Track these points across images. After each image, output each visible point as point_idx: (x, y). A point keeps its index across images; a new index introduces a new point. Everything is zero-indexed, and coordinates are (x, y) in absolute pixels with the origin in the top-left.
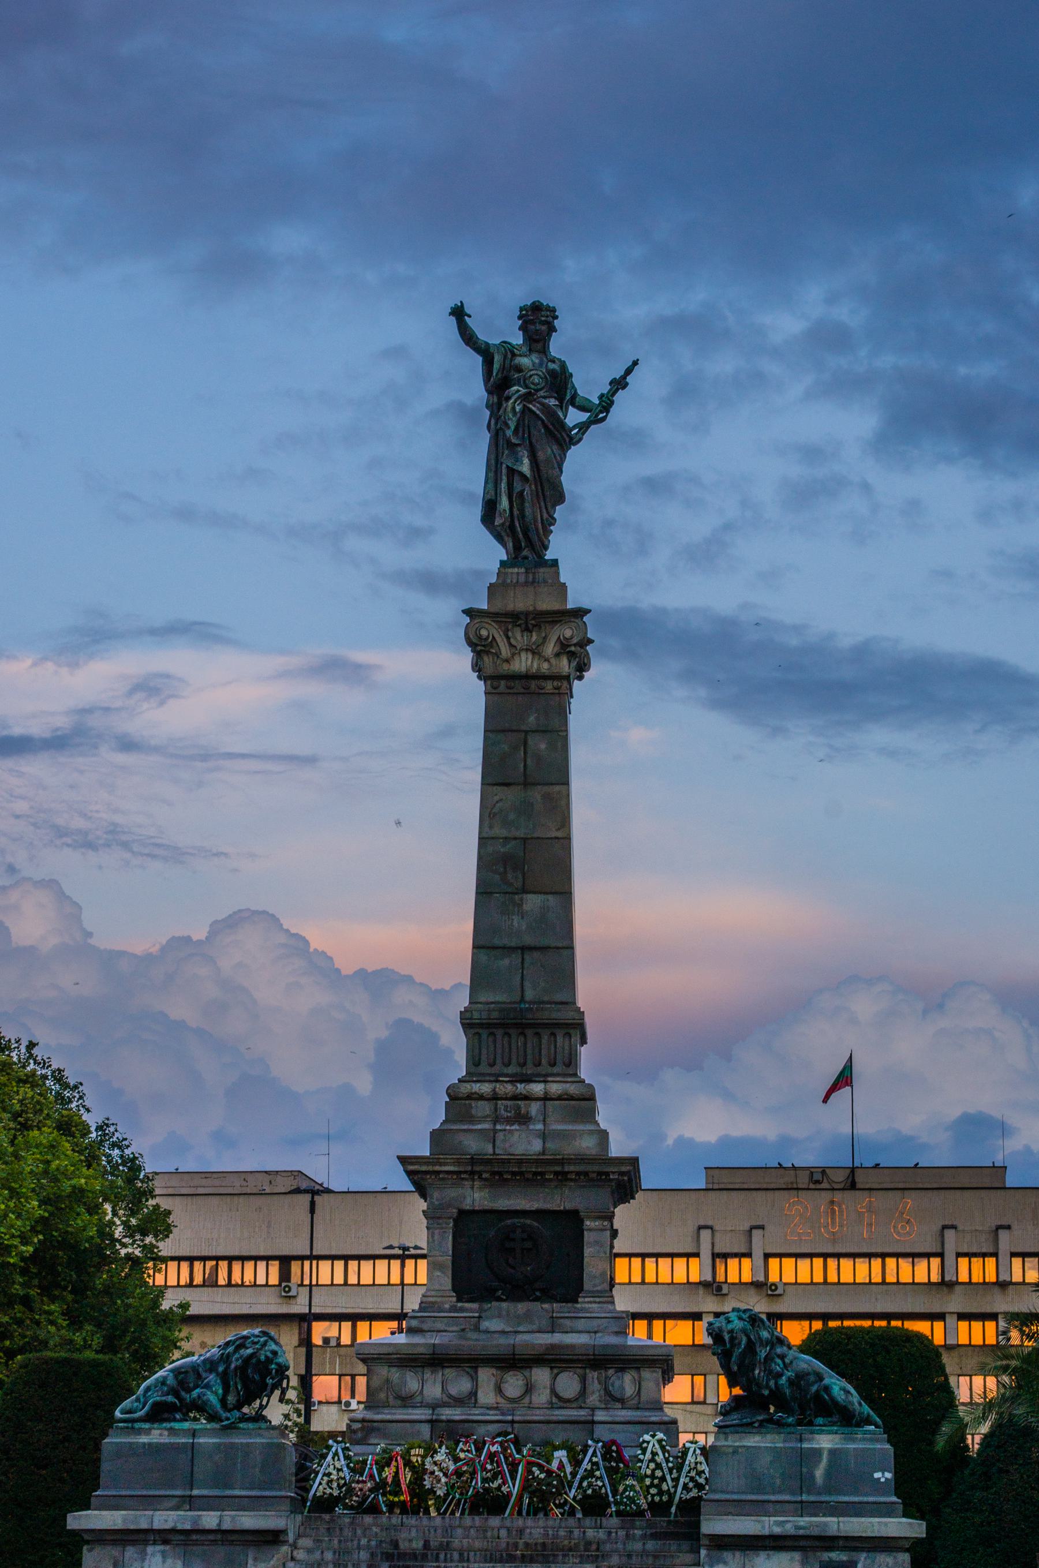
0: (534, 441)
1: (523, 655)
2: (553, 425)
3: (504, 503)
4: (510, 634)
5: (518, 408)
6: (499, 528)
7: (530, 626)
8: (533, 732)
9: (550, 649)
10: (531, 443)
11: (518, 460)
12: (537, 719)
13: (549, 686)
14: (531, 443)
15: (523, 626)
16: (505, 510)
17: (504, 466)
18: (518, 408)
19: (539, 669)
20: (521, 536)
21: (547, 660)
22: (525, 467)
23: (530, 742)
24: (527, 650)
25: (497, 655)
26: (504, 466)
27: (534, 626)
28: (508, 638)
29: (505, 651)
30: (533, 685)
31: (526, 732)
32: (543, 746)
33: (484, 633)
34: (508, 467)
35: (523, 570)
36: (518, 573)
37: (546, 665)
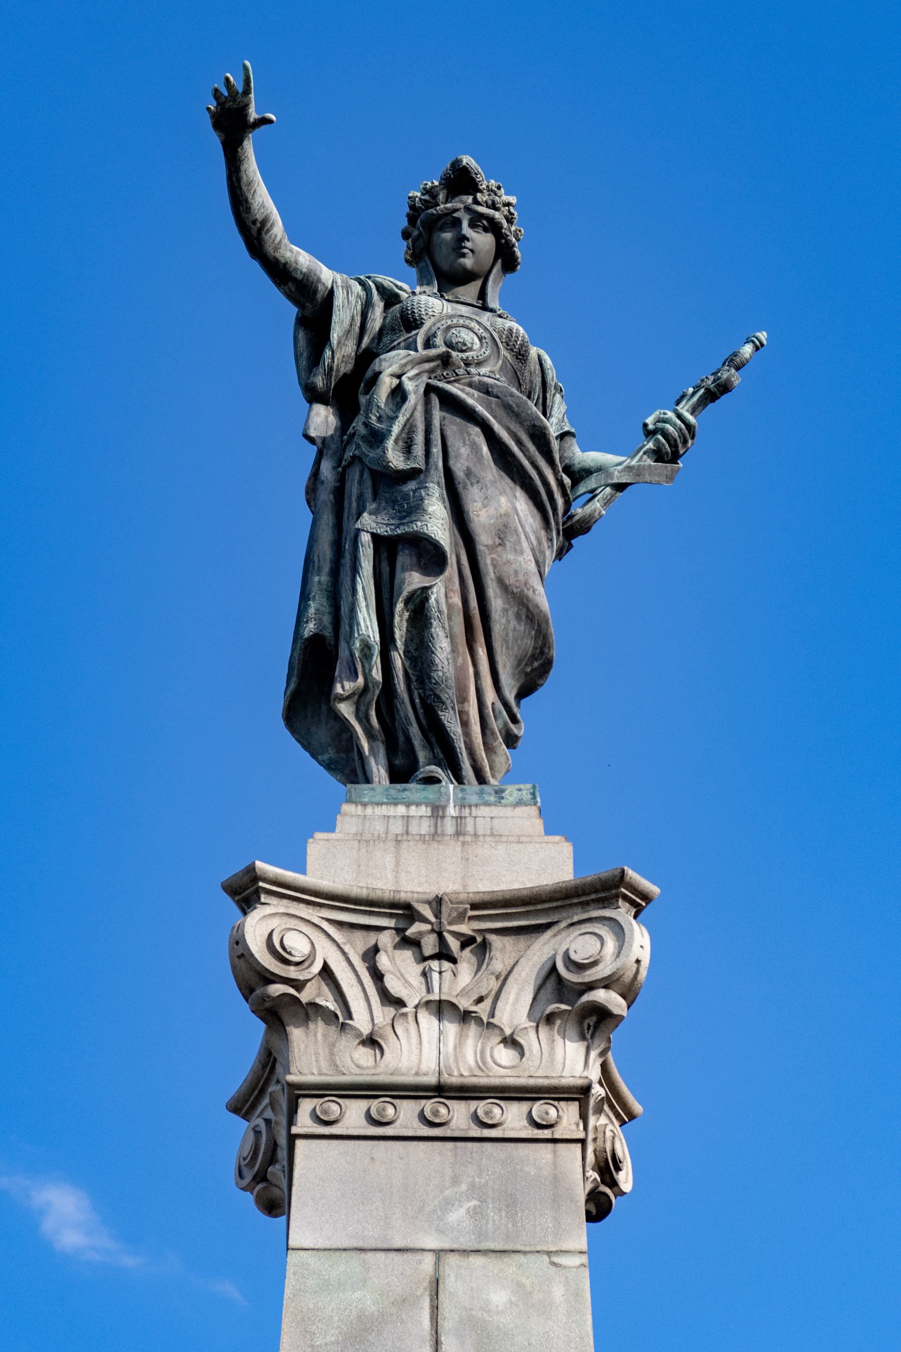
0: (458, 468)
1: (428, 1021)
2: (519, 442)
3: (367, 624)
4: (383, 961)
5: (413, 387)
6: (346, 710)
7: (454, 944)
8: (465, 1252)
9: (515, 1008)
10: (449, 474)
11: (413, 509)
12: (476, 1214)
13: (513, 1118)
14: (449, 474)
15: (430, 945)
16: (367, 647)
17: (366, 538)
18: (413, 387)
19: (481, 1066)
20: (414, 730)
21: (511, 1042)
22: (436, 522)
23: (451, 1283)
24: (441, 1008)
25: (340, 1019)
26: (366, 538)
27: (467, 942)
28: (377, 976)
29: (365, 1012)
30: (459, 1116)
31: (439, 1253)
32: (499, 1297)
33: (297, 945)
34: (375, 537)
35: (424, 811)
36: (407, 818)
37: (505, 1055)
